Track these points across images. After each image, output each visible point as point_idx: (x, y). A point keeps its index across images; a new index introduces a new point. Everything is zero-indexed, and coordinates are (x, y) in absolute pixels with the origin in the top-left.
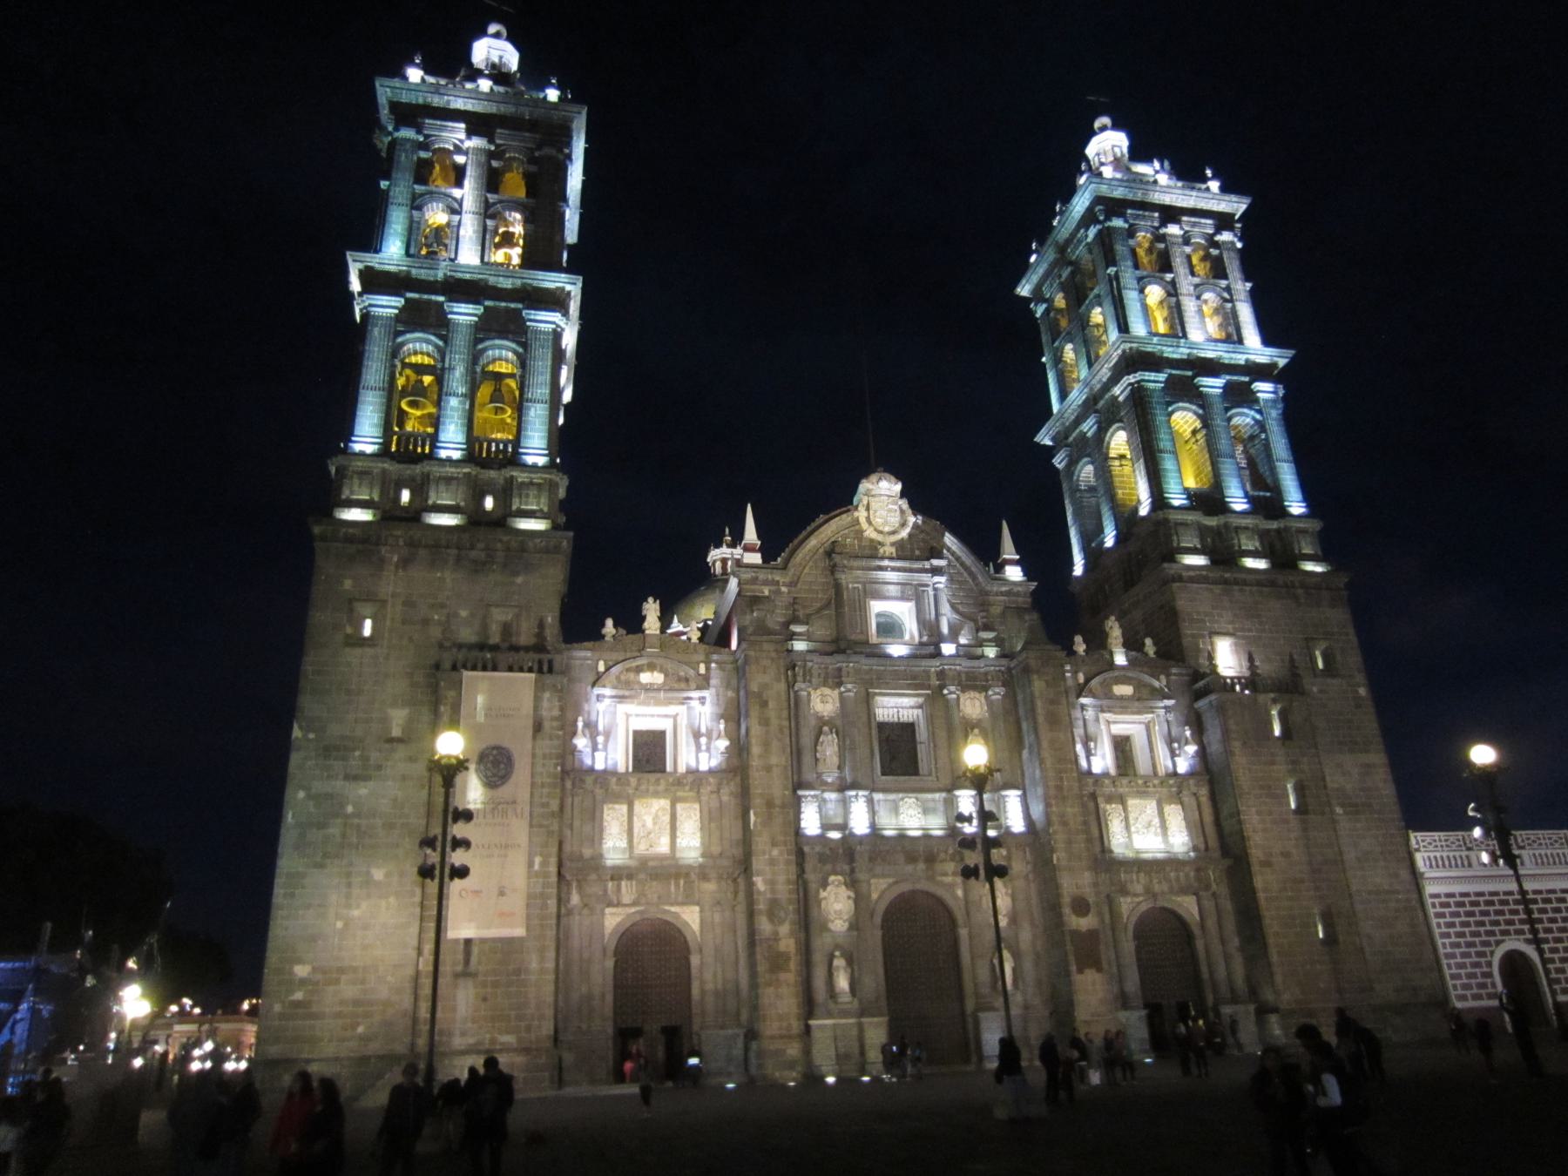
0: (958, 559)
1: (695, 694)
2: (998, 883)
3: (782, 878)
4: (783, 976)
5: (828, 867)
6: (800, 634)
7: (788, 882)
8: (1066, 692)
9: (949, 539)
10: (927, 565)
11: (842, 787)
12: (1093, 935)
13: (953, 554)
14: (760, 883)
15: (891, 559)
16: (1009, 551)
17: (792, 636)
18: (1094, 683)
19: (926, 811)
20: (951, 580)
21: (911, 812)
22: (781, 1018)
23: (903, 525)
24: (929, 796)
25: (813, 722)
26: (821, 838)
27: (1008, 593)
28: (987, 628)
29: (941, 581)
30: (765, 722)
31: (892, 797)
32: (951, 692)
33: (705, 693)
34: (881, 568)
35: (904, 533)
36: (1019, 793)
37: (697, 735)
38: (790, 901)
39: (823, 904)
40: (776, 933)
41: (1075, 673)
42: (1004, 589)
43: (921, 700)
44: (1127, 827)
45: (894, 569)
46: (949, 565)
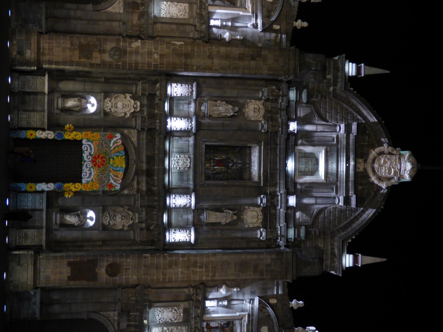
0: (357, 218)
1: (260, 22)
2: (133, 204)
3: (139, 59)
4: (77, 52)
5: (145, 102)
6: (301, 97)
7: (137, 63)
8: (263, 279)
9: (370, 212)
10: (351, 192)
11: (198, 115)
12: (94, 277)
13: (360, 215)
14: (137, 44)
15: (355, 166)
16: (363, 260)
17: (299, 94)
18: (270, 309)
19: (181, 173)
20: (341, 211)
21: (181, 163)
22: (50, 49)
23: (380, 179)
24: (191, 177)
25: (241, 101)
26: (165, 96)
27: (333, 254)
28: (308, 233)
29: (341, 204)
30: (241, 57)
31: (191, 150)
32: (262, 200)
33: (260, 29)
34: (348, 161)
35: (374, 179)
36: (192, 241)
37: (234, 19)
38: (124, 63)
39: (122, 96)
40: (104, 52)
41: (277, 297)
42: (336, 251)
43: (256, 179)
44: (166, 324)
45: (348, 168)
46: (352, 210)
